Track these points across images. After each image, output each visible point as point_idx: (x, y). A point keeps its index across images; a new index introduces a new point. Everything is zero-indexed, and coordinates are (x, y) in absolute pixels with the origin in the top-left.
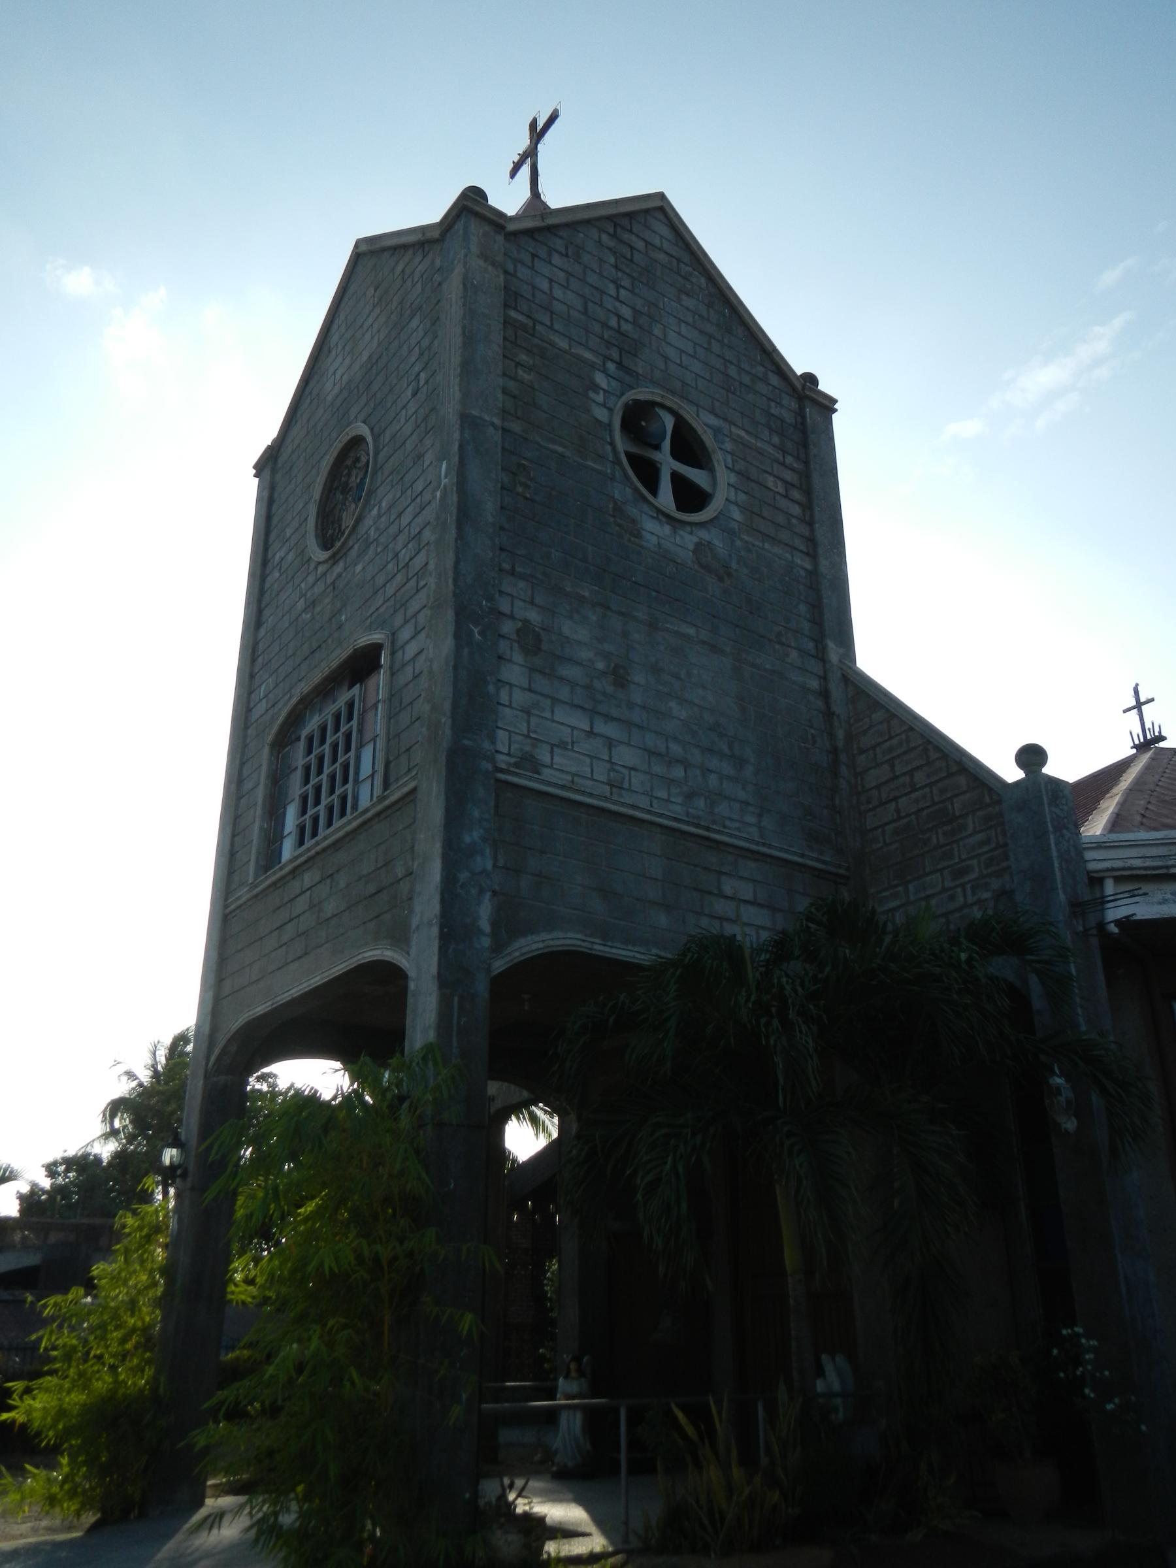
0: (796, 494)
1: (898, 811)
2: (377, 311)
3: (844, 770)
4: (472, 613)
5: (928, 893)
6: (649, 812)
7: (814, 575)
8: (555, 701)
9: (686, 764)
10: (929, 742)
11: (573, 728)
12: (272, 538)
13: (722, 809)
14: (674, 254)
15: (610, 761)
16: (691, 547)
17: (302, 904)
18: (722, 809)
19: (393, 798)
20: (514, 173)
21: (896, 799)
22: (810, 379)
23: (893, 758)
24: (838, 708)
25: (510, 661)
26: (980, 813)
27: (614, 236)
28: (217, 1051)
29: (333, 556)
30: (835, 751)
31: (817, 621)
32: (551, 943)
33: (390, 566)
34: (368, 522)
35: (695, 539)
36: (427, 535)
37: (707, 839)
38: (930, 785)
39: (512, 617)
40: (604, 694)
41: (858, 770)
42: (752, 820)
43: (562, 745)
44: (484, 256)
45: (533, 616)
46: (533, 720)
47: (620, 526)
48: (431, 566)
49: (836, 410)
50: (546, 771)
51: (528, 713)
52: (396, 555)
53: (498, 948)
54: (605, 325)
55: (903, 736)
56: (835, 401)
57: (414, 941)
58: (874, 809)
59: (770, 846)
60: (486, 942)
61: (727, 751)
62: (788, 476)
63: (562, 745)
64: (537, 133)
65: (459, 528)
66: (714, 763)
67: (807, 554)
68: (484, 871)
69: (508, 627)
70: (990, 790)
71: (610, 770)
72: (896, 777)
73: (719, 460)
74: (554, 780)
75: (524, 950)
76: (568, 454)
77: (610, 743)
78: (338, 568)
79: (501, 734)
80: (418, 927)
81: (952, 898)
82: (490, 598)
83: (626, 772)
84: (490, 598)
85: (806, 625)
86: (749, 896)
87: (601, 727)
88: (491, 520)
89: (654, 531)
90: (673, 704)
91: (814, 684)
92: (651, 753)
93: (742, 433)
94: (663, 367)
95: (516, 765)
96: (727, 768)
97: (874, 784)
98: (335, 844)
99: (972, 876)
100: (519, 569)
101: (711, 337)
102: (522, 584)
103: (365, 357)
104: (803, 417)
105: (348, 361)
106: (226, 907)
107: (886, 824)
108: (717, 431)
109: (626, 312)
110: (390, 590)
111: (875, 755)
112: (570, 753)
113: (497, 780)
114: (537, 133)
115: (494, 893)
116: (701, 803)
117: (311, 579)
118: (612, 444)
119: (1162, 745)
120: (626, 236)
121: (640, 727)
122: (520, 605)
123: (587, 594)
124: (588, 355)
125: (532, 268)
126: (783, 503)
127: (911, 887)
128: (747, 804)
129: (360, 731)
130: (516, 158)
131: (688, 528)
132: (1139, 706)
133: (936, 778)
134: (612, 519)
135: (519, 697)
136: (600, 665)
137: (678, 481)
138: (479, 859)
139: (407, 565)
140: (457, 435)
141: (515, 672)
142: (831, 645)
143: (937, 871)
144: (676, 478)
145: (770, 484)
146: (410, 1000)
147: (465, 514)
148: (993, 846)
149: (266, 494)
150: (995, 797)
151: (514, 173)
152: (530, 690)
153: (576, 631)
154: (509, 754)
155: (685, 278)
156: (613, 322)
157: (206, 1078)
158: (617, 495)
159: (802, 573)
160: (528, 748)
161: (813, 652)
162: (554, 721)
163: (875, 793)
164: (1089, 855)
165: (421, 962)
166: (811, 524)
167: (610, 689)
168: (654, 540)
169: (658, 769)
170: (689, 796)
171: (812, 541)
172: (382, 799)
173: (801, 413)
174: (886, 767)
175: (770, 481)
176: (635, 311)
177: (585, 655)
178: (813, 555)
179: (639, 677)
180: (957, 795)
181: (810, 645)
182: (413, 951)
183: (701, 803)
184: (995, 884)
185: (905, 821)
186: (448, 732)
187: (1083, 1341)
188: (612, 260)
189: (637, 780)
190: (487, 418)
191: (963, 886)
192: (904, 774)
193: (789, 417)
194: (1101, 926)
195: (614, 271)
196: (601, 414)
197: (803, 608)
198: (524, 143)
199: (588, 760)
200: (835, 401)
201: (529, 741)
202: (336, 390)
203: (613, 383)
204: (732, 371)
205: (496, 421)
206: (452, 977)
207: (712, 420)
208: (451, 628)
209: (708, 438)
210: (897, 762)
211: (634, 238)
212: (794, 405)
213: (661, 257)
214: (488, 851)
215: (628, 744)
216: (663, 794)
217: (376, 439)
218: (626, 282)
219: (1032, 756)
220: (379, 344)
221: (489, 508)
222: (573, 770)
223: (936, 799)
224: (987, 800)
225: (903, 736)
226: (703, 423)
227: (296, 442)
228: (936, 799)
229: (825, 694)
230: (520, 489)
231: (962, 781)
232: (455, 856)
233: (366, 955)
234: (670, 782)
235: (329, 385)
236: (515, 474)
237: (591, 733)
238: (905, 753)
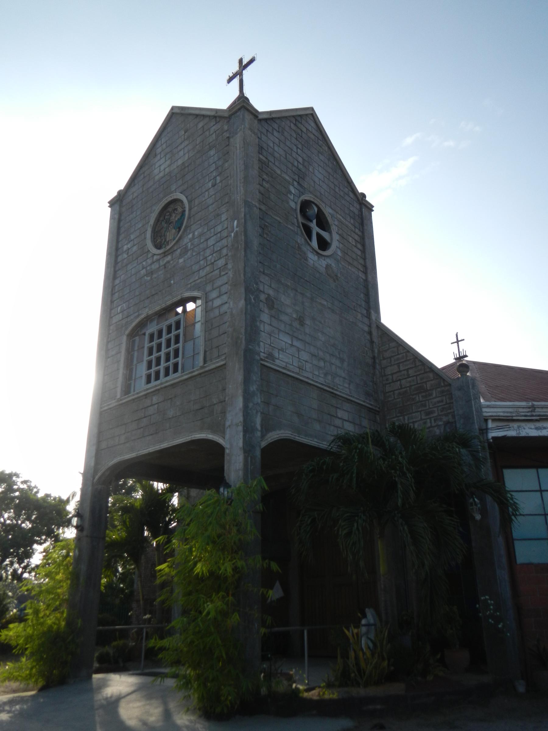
0: (359, 246)
1: (401, 385)
2: (187, 142)
3: (378, 367)
4: (251, 291)
5: (414, 420)
6: (313, 380)
7: (366, 281)
8: (280, 330)
9: (325, 361)
10: (416, 358)
11: (286, 343)
12: (120, 239)
13: (337, 380)
14: (316, 135)
15: (298, 358)
16: (324, 266)
17: (151, 410)
18: (337, 380)
20: (230, 80)
21: (400, 380)
22: (363, 195)
23: (399, 363)
24: (375, 340)
25: (263, 312)
26: (439, 389)
27: (295, 125)
28: (99, 474)
29: (164, 253)
30: (374, 358)
31: (367, 302)
32: (281, 435)
33: (202, 262)
34: (186, 240)
35: (326, 263)
36: (225, 251)
37: (332, 393)
38: (416, 376)
39: (264, 292)
40: (296, 328)
41: (383, 366)
42: (347, 385)
43: (282, 350)
44: (250, 129)
45: (271, 292)
46: (272, 338)
47: (300, 255)
48: (230, 266)
49: (373, 211)
50: (277, 361)
51: (270, 335)
52: (205, 258)
53: (263, 436)
54: (293, 165)
55: (404, 354)
56: (373, 207)
57: (228, 432)
58: (389, 383)
59: (354, 397)
60: (259, 434)
61: (338, 356)
62: (356, 237)
63: (282, 350)
64: (243, 66)
65: (245, 251)
66: (334, 360)
67: (363, 272)
68: (257, 403)
69: (263, 297)
70: (444, 380)
71: (299, 361)
72: (400, 371)
73: (334, 229)
74: (280, 365)
75: (272, 438)
76: (281, 221)
77: (299, 350)
78: (169, 258)
79: (261, 344)
80: (229, 426)
81: (425, 423)
82: (257, 284)
83: (304, 362)
84: (257, 284)
85: (363, 304)
86: (346, 419)
87: (296, 343)
88: (256, 249)
89: (312, 258)
90: (319, 334)
91: (366, 329)
92: (313, 355)
93: (341, 218)
94: (313, 185)
95: (267, 358)
96: (338, 363)
97: (390, 373)
98: (172, 385)
99: (436, 414)
100: (266, 271)
101: (329, 173)
102: (267, 278)
103: (180, 162)
104: (362, 213)
105: (168, 162)
106: (101, 408)
107: (395, 390)
108: (332, 216)
109: (300, 160)
110: (202, 273)
111: (391, 361)
112: (285, 354)
113: (261, 364)
114: (243, 66)
115: (261, 413)
116: (329, 377)
117: (149, 261)
118: (297, 218)
119: (466, 359)
120: (299, 125)
121: (308, 343)
122: (267, 287)
123: (289, 284)
124: (287, 178)
125: (267, 136)
126: (355, 249)
127: (406, 417)
128: (345, 378)
129: (185, 335)
130: (231, 75)
131: (323, 258)
132: (458, 342)
133: (419, 373)
134: (297, 252)
135: (267, 328)
136: (294, 316)
137: (319, 236)
138: (256, 398)
139: (212, 264)
140: (243, 210)
141: (265, 317)
142: (372, 312)
143: (418, 412)
144: (318, 235)
145: (350, 241)
146: (226, 458)
147: (247, 245)
148: (444, 403)
149: (117, 216)
150: (446, 383)
151: (230, 80)
152: (271, 325)
153: (286, 299)
154: (264, 353)
155: (320, 146)
156: (296, 164)
157: (93, 485)
158: (299, 242)
159: (362, 280)
160: (270, 351)
161: (366, 315)
162: (279, 339)
163: (390, 377)
164: (484, 410)
165: (233, 442)
166: (365, 259)
167: (298, 326)
168: (312, 262)
169: (315, 362)
170: (326, 374)
171: (365, 266)
172: (202, 367)
173: (361, 210)
174: (396, 366)
175: (350, 239)
176: (303, 159)
177: (289, 311)
178: (365, 273)
179: (308, 322)
180: (429, 381)
181: (365, 312)
182: (227, 436)
183: (329, 377)
184: (445, 419)
185: (404, 390)
186: (244, 342)
187: (489, 601)
188: (295, 136)
189: (308, 366)
190: (254, 203)
191: (430, 418)
192: (404, 370)
193: (357, 212)
194: (488, 440)
195: (295, 140)
196: (292, 205)
197: (362, 295)
198: (236, 68)
199: (291, 357)
200: (373, 207)
201: (271, 347)
202: (162, 174)
203: (297, 191)
204: (337, 190)
205: (257, 205)
206: (248, 448)
207: (331, 211)
208: (243, 296)
209: (329, 219)
210: (401, 365)
211: (302, 126)
212: (358, 207)
213: (312, 136)
214: (259, 394)
215: (304, 351)
216: (317, 373)
217: (190, 202)
218: (300, 146)
220: (189, 159)
221: (255, 242)
222: (286, 360)
223: (419, 382)
224: (442, 384)
225: (404, 354)
226: (327, 211)
227: (135, 195)
228: (419, 382)
229: (370, 333)
230: (265, 236)
231: (431, 375)
232: (247, 397)
233: (196, 436)
234: (319, 368)
235: (156, 171)
236: (263, 229)
237: (292, 345)
238: (405, 361)
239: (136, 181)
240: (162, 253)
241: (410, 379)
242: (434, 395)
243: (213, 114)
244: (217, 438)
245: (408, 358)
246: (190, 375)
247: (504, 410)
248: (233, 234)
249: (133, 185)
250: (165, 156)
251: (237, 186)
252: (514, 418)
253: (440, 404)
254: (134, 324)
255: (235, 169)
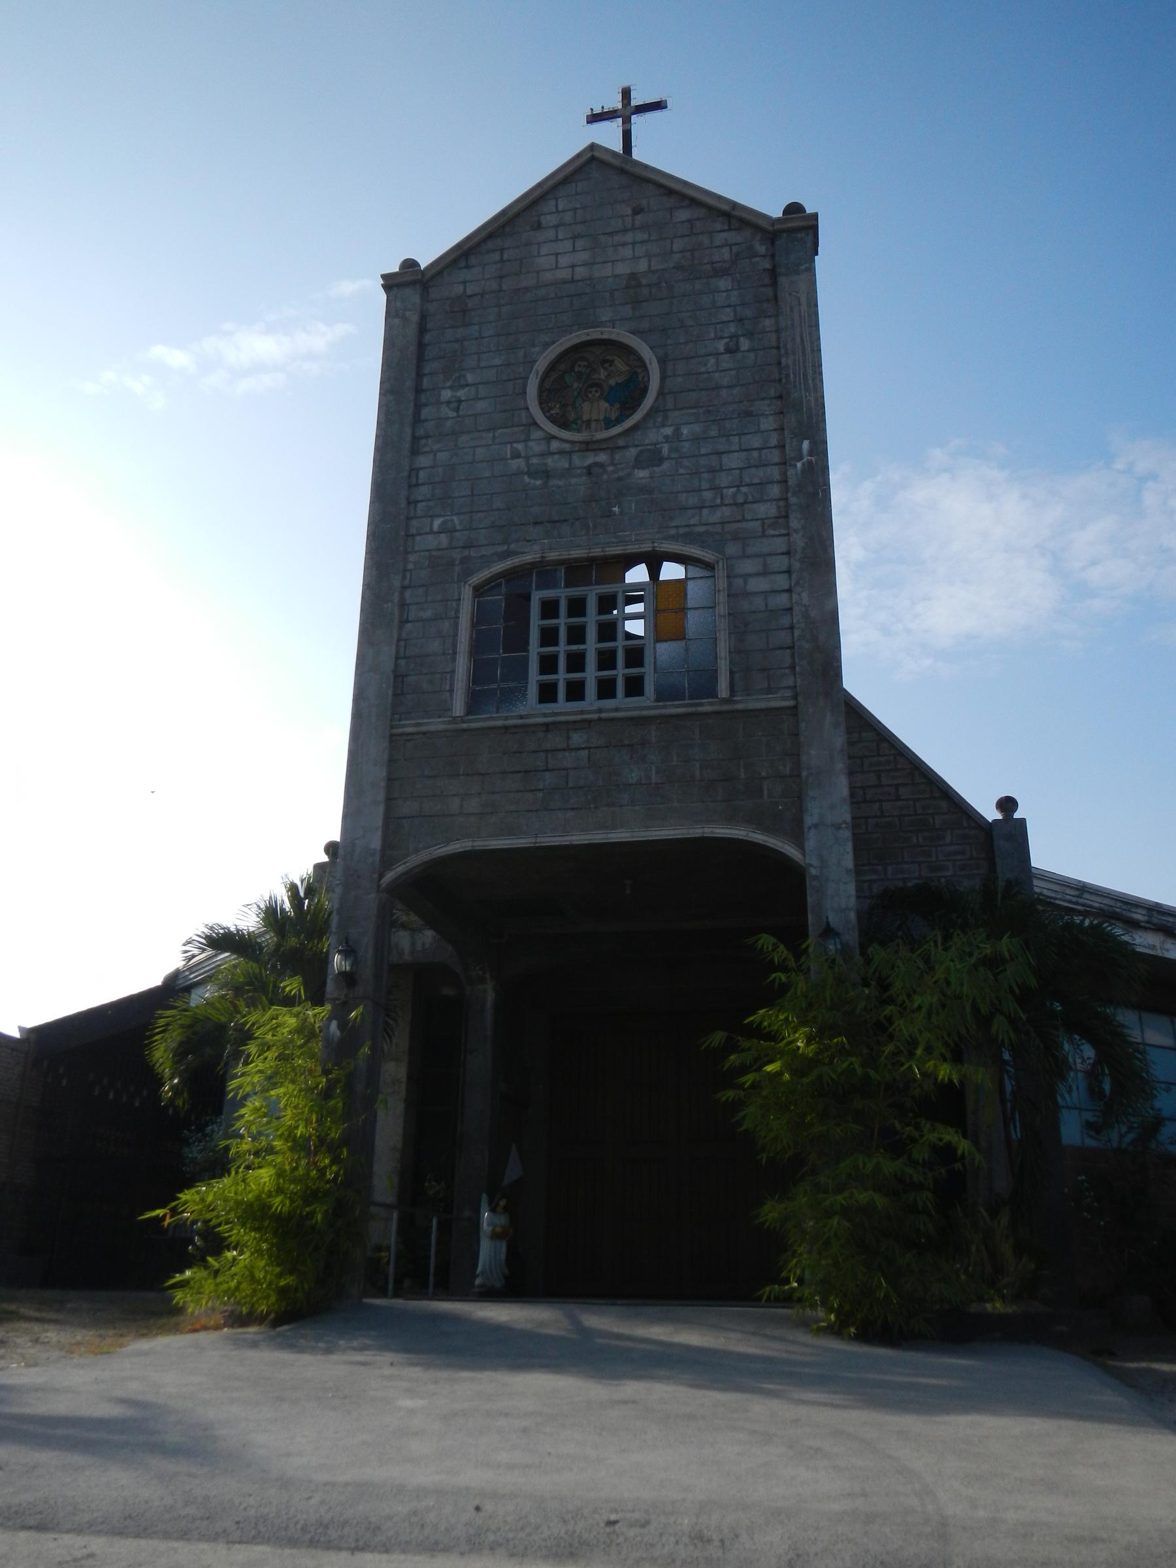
2: (641, 236)
19: (740, 706)
21: (880, 801)
29: (587, 443)
80: (816, 826)
98: (632, 719)
99: (949, 873)
127: (890, 869)
130: (598, 110)
164: (1036, 882)
182: (811, 843)
217: (663, 361)
219: (1007, 805)
224: (965, 824)
231: (944, 804)
233: (706, 830)
239: (473, 260)
240: (580, 442)
241: (899, 803)
242: (948, 840)
243: (726, 208)
244: (780, 844)
245: (899, 766)
246: (689, 710)
247: (1057, 888)
248: (799, 465)
249: (462, 263)
250: (574, 238)
251: (805, 375)
252: (1058, 902)
253: (959, 857)
254: (498, 567)
255: (798, 340)
